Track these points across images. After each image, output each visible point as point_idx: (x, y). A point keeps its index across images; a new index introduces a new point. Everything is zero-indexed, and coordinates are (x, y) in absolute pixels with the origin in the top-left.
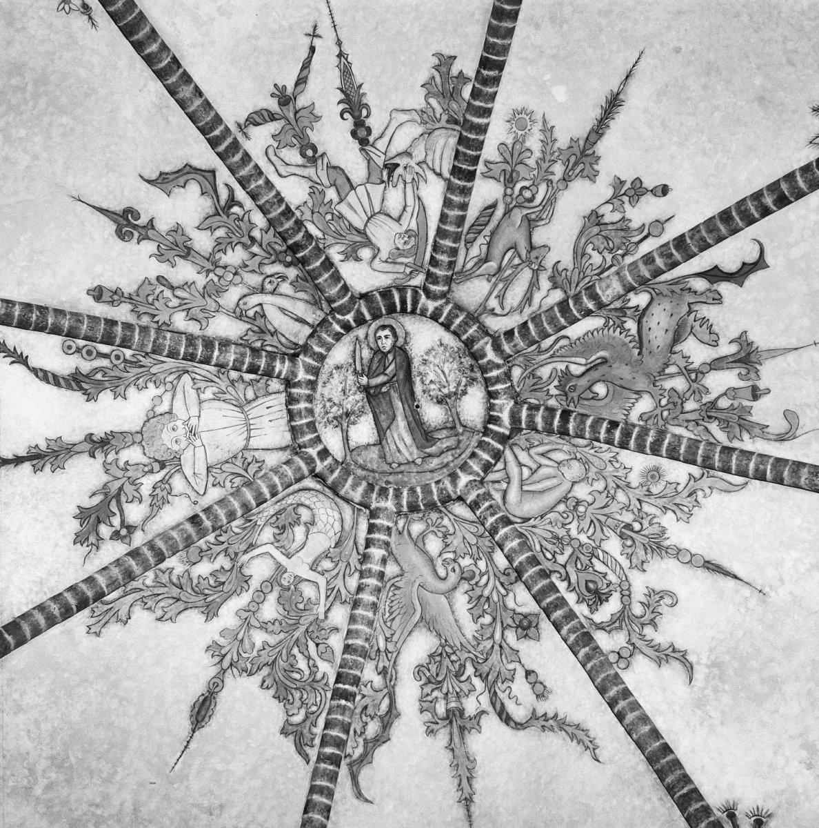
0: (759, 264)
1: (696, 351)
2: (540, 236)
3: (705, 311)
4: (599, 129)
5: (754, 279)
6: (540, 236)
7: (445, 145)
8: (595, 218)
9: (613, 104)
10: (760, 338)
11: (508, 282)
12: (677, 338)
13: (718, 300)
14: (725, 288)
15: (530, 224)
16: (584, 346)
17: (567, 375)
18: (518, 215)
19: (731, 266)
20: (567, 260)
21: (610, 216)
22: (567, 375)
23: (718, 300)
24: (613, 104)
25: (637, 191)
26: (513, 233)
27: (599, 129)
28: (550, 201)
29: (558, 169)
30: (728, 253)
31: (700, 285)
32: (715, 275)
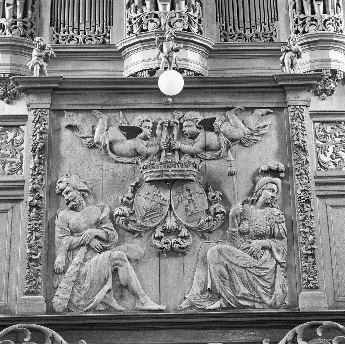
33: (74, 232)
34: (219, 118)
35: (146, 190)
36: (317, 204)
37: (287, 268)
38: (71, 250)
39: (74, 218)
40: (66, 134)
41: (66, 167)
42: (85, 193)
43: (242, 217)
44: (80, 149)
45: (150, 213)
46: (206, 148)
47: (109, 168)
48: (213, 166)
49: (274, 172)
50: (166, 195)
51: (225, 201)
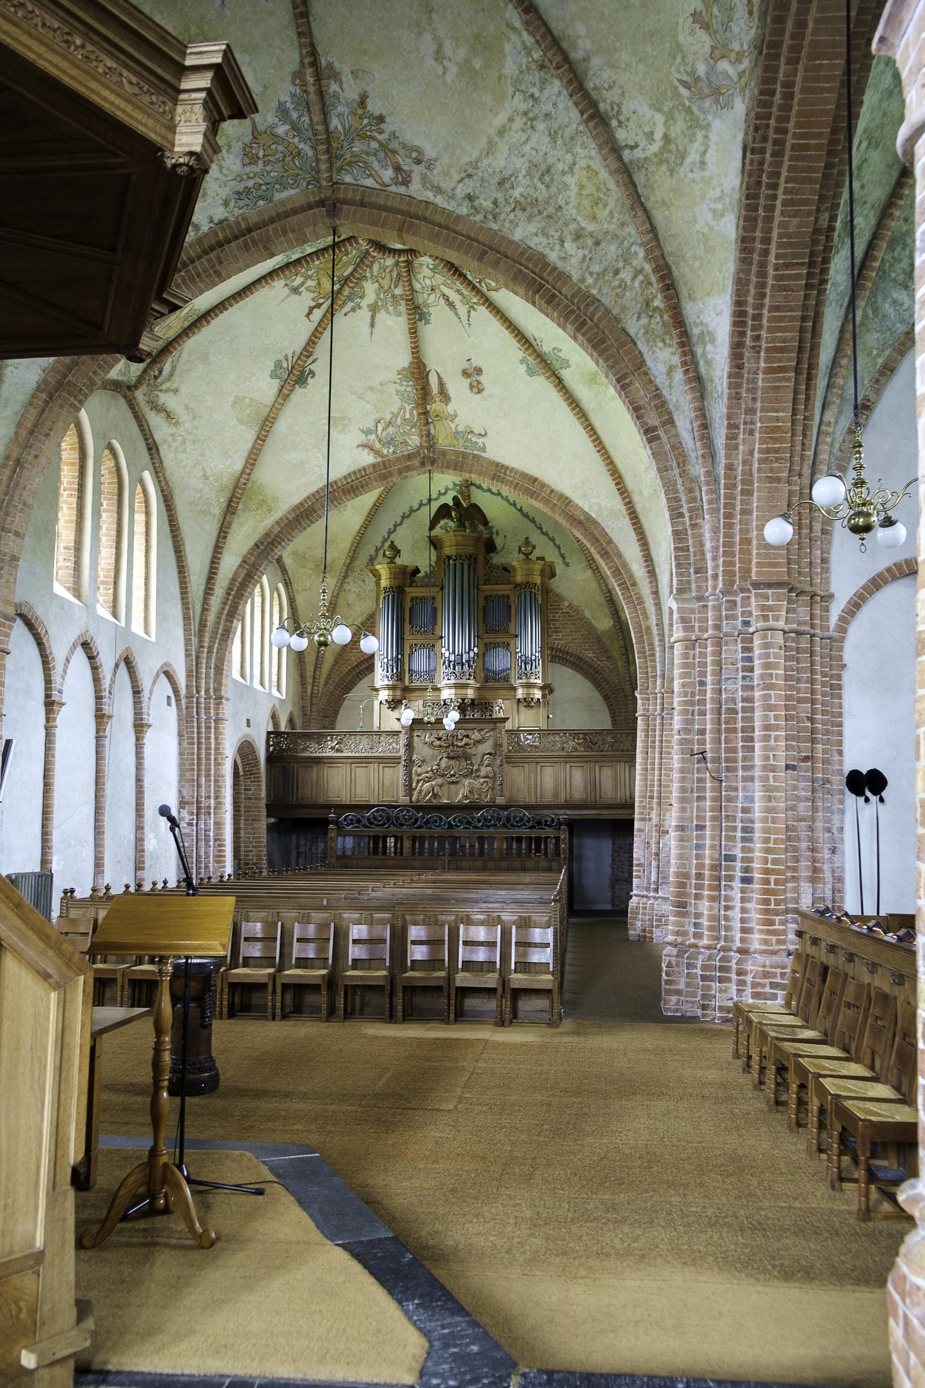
0: (308, 315)
1: (310, 283)
2: (377, 285)
3: (315, 295)
4: (373, 318)
5: (307, 310)
6: (377, 285)
7: (420, 299)
8: (362, 297)
9: (372, 325)
10: (295, 297)
11: (380, 268)
12: (319, 283)
13: (313, 299)
14: (313, 304)
15: (381, 287)
16: (346, 266)
17: (347, 255)
18: (386, 288)
19: (315, 310)
20: (364, 284)
21: (359, 300)
22: (347, 255)
23: (313, 299)
24: (372, 325)
25: (353, 310)
26: (386, 283)
27: (373, 318)
28: (378, 295)
29: (380, 303)
30: (318, 314)
31: (321, 301)
32: (318, 306)
33: (419, 775)
34: (469, 733)
35: (445, 760)
36: (506, 765)
37: (493, 789)
38: (418, 781)
39: (419, 770)
40: (416, 738)
41: (416, 751)
42: (423, 761)
43: (478, 770)
44: (421, 745)
45: (448, 768)
46: (466, 744)
47: (431, 751)
48: (469, 751)
49: (490, 754)
50: (452, 762)
51: (472, 764)
